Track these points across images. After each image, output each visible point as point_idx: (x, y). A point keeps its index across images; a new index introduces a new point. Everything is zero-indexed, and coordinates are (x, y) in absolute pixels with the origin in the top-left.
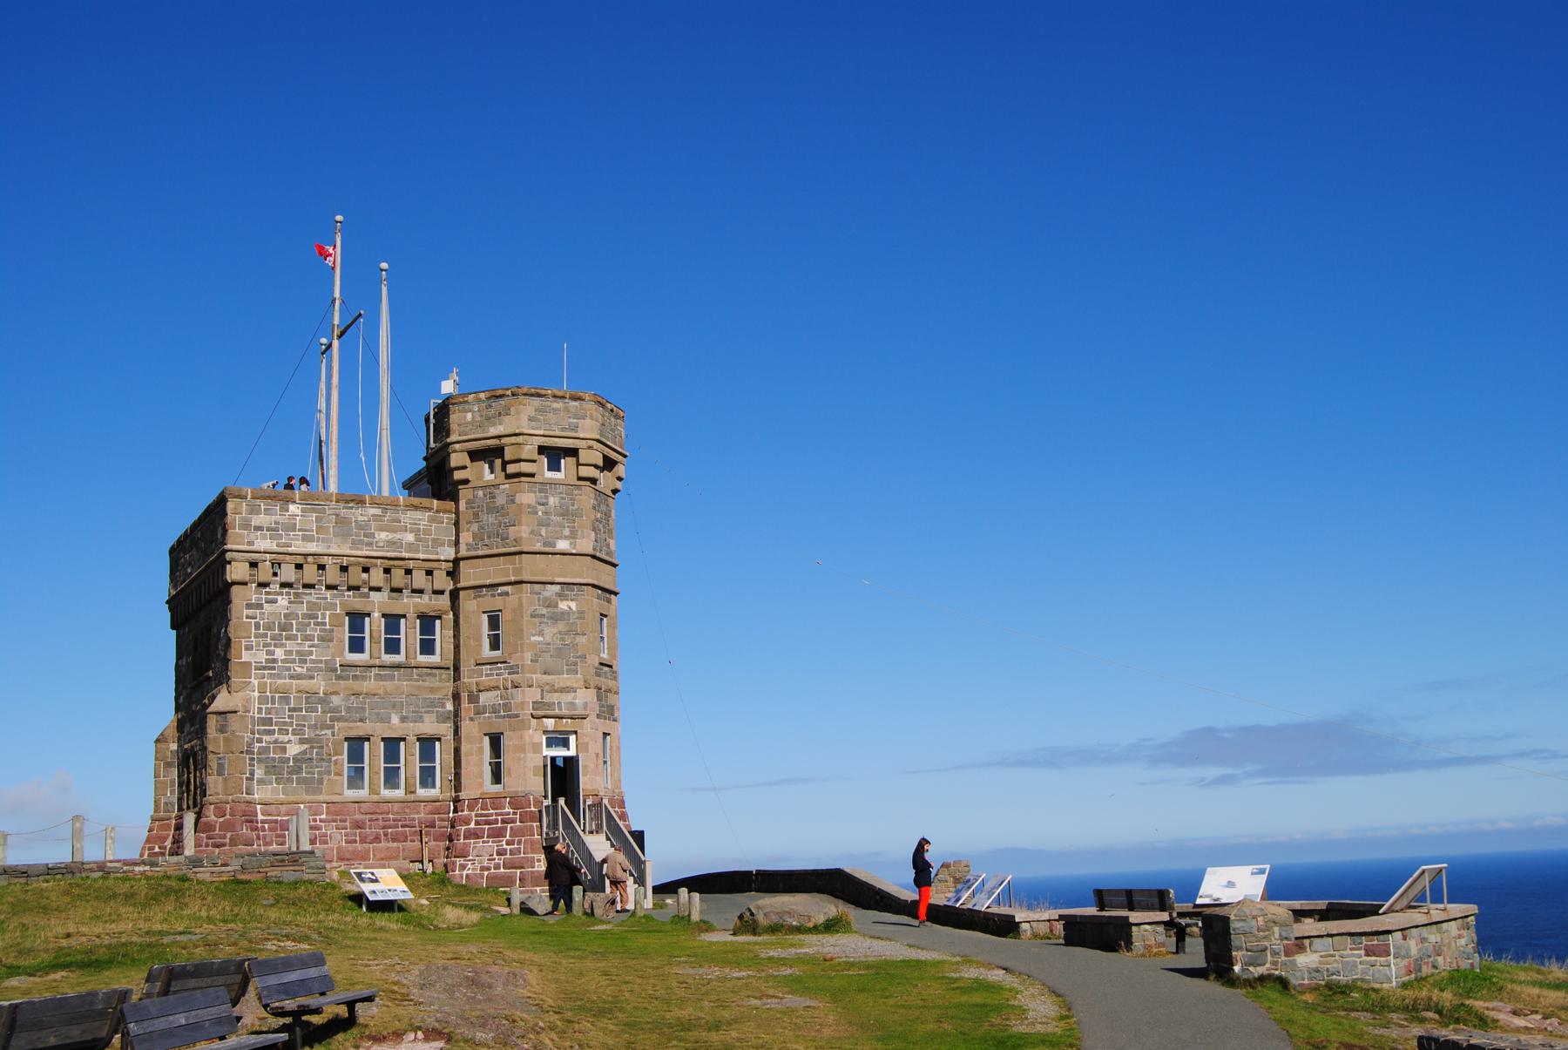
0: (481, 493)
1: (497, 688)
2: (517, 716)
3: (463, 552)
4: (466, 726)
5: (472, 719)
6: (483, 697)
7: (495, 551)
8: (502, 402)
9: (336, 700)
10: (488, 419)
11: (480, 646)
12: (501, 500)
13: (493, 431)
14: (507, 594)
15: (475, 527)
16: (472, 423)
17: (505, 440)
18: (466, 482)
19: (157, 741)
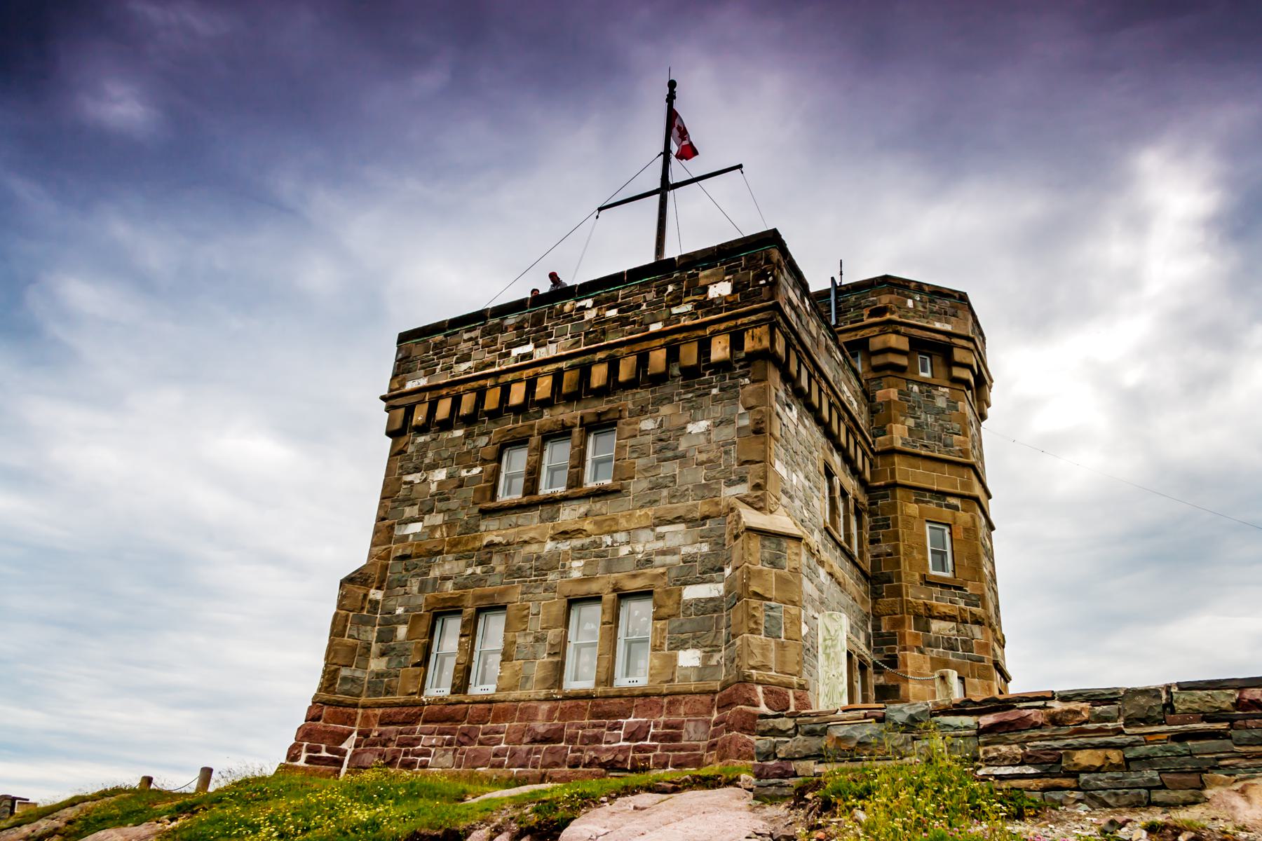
0: (916, 388)
1: (952, 618)
2: (981, 660)
3: (898, 444)
4: (912, 660)
5: (922, 652)
6: (936, 625)
7: (936, 454)
8: (947, 302)
9: (822, 572)
10: (932, 312)
11: (926, 560)
12: (941, 403)
13: (938, 325)
14: (956, 508)
15: (911, 422)
16: (915, 309)
17: (955, 341)
18: (902, 369)
19: (349, 581)
